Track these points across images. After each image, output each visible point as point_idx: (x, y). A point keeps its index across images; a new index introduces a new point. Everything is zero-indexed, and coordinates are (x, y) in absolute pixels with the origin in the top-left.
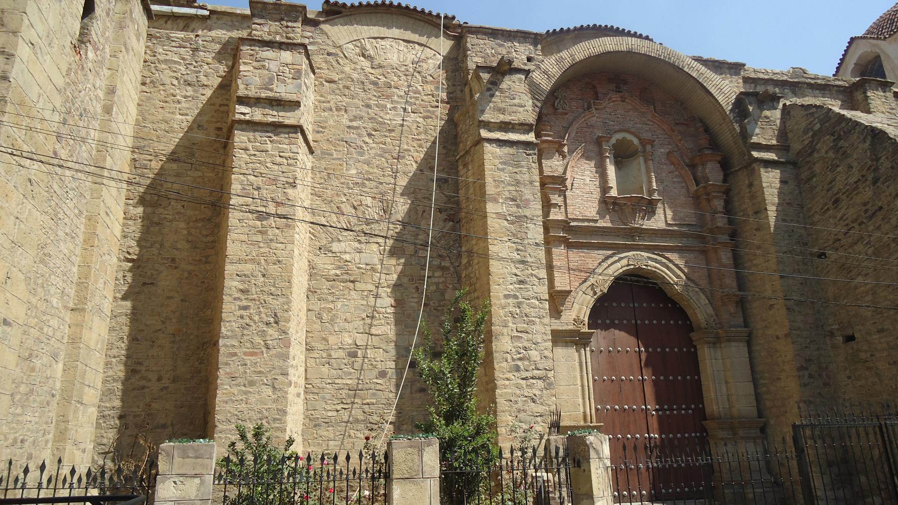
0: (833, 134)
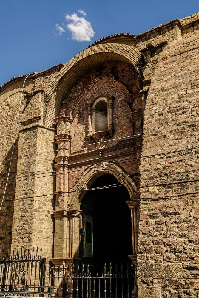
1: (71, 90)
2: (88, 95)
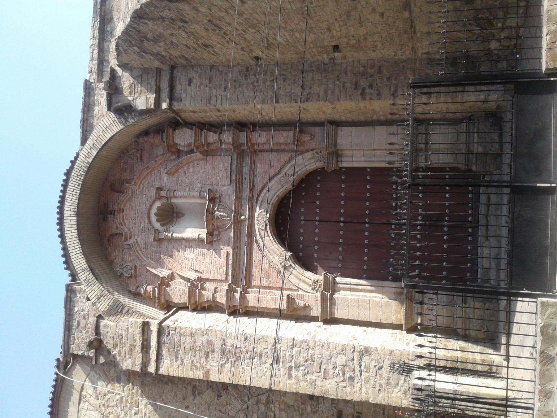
0: (142, 41)
1: (119, 274)
2: (139, 240)
